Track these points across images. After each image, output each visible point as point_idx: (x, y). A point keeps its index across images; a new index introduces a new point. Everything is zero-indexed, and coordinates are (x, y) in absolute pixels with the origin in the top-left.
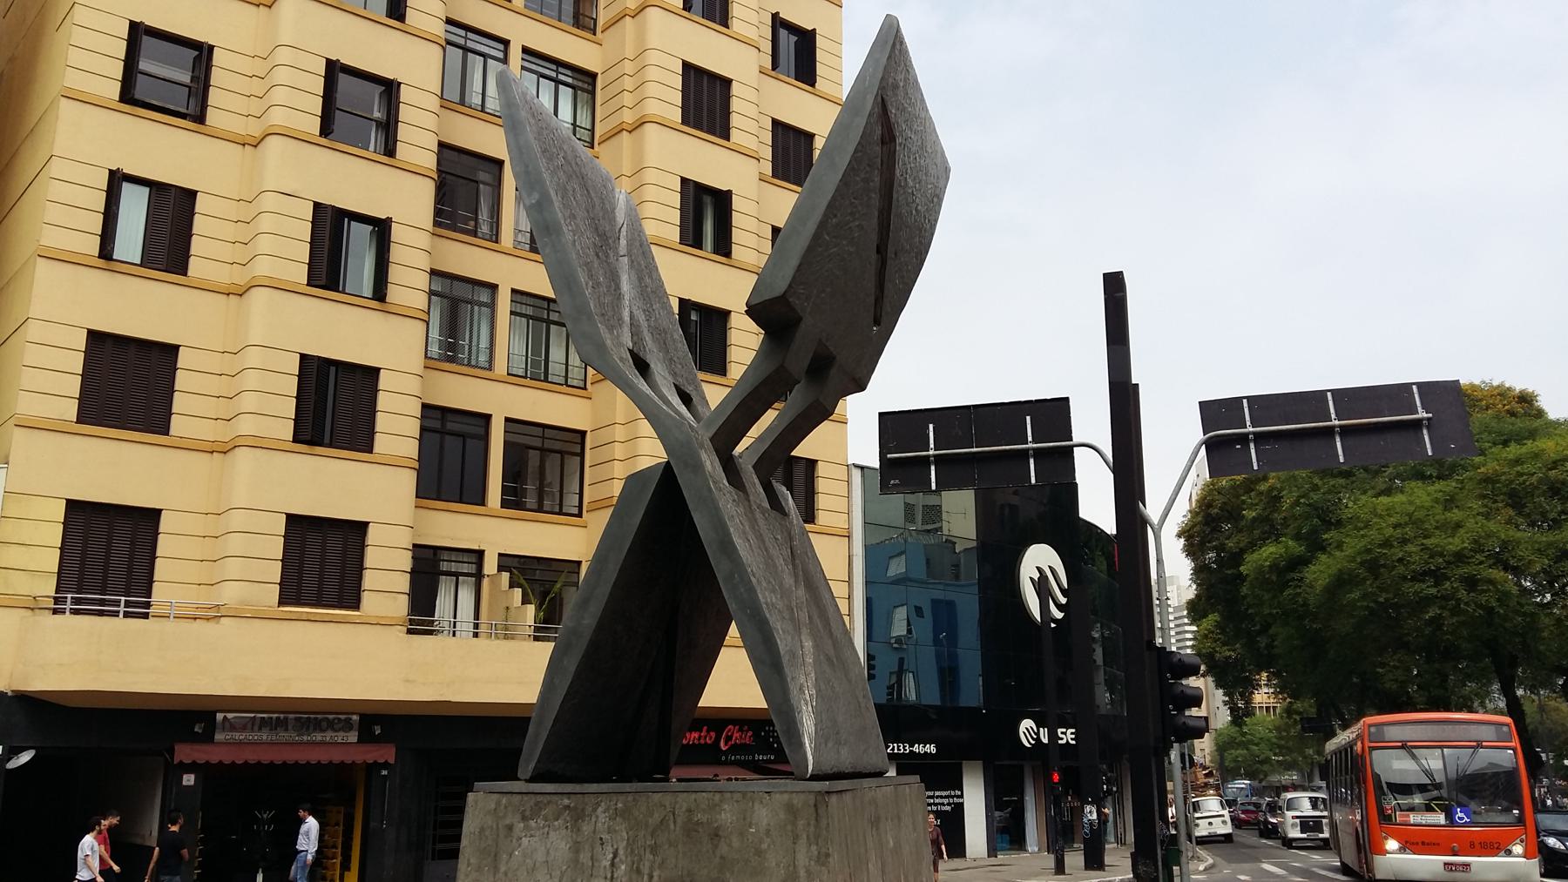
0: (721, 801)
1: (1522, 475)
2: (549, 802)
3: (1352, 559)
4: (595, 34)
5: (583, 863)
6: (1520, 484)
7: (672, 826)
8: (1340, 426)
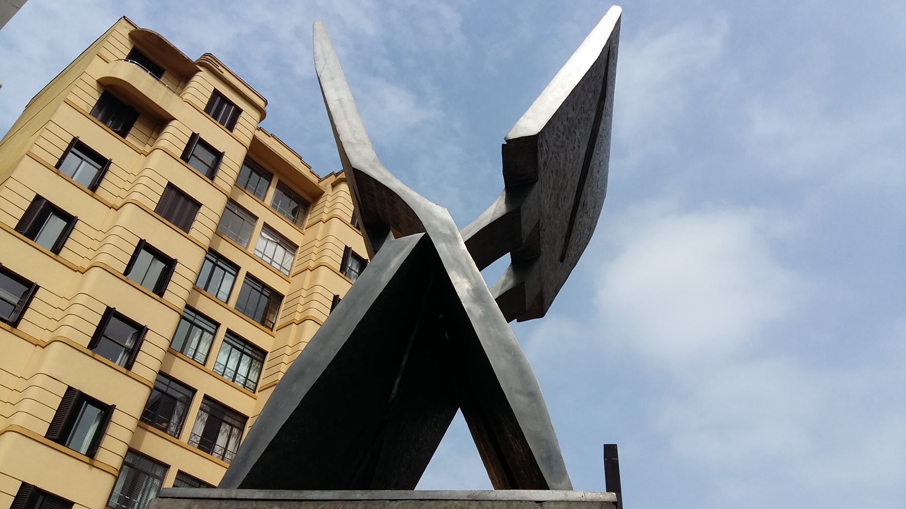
4: (272, 331)
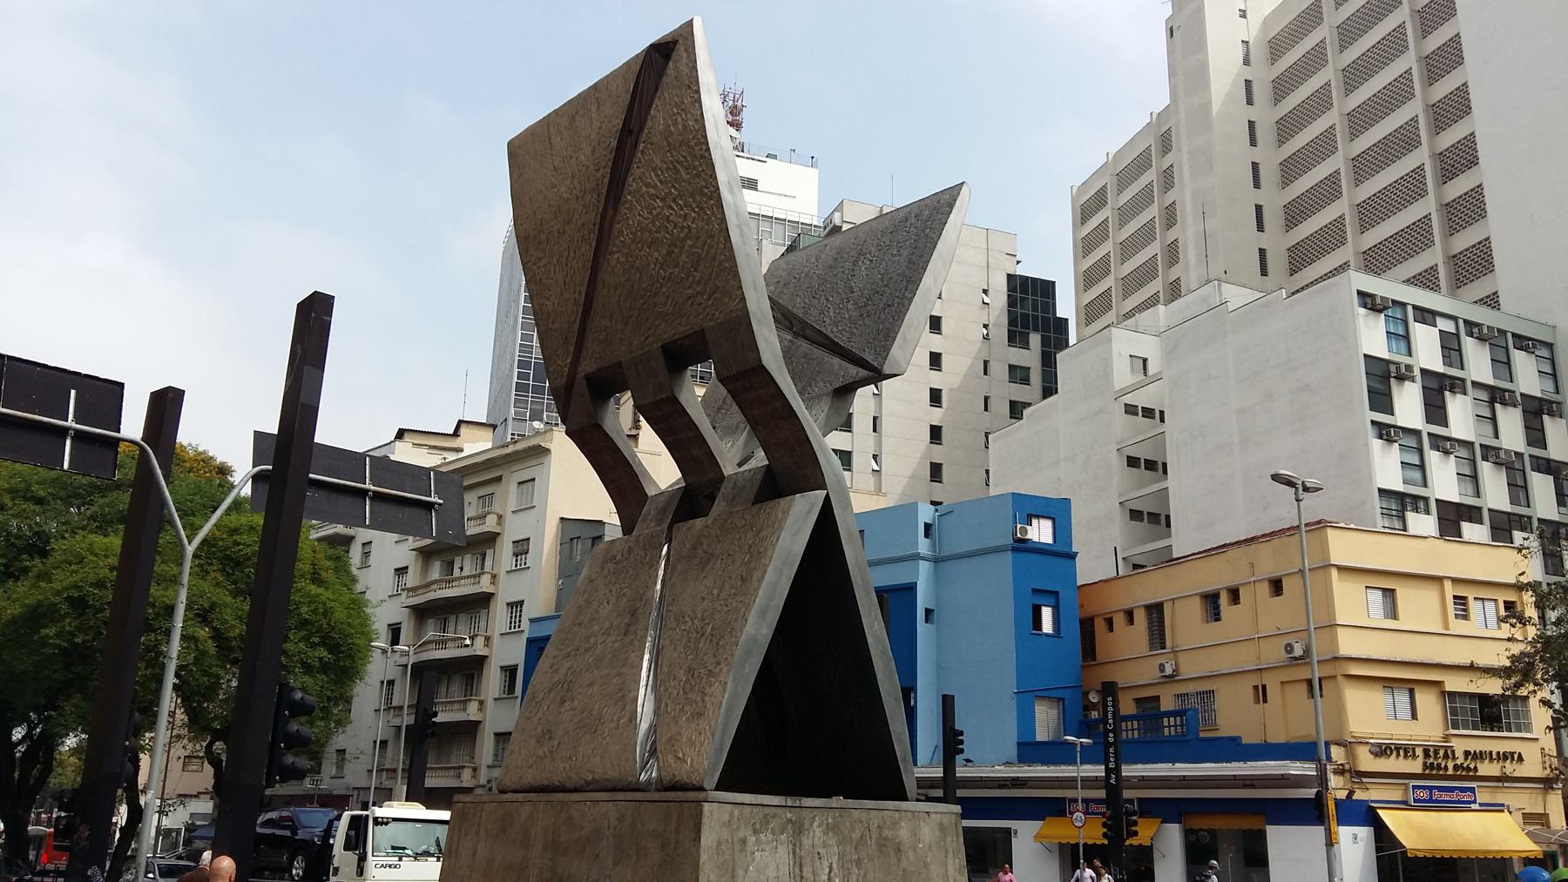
0: (900, 819)
1: (239, 544)
2: (775, 815)
3: (58, 593)
5: (807, 879)
6: (234, 553)
7: (869, 842)
8: (374, 492)
